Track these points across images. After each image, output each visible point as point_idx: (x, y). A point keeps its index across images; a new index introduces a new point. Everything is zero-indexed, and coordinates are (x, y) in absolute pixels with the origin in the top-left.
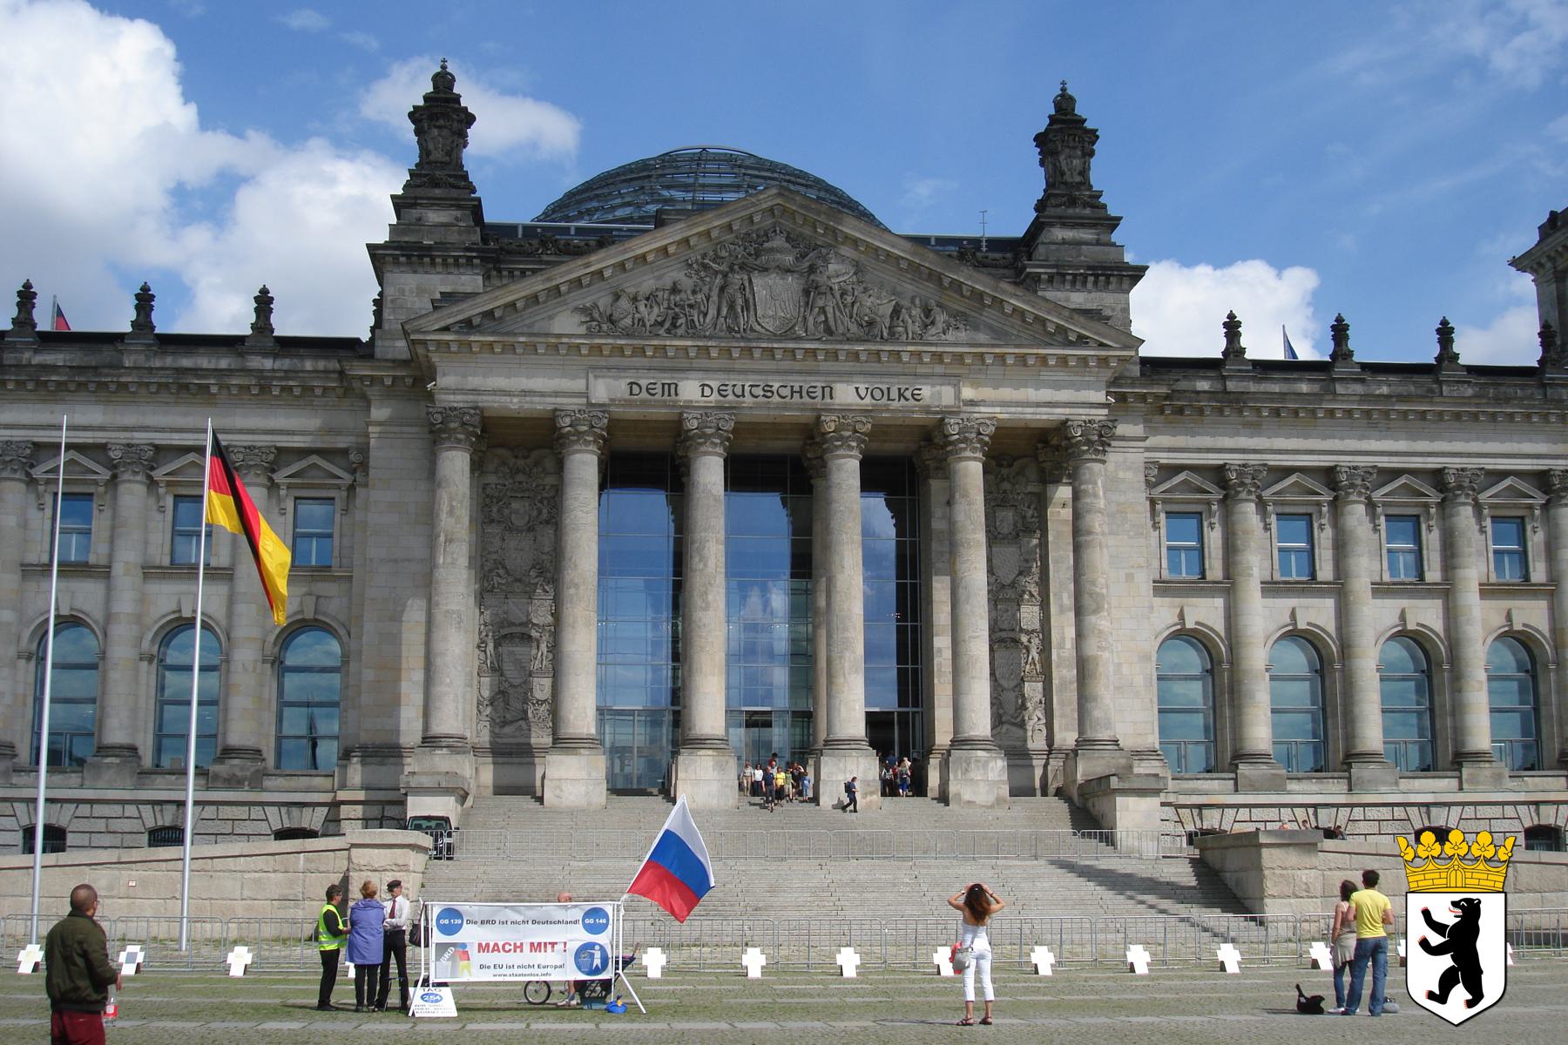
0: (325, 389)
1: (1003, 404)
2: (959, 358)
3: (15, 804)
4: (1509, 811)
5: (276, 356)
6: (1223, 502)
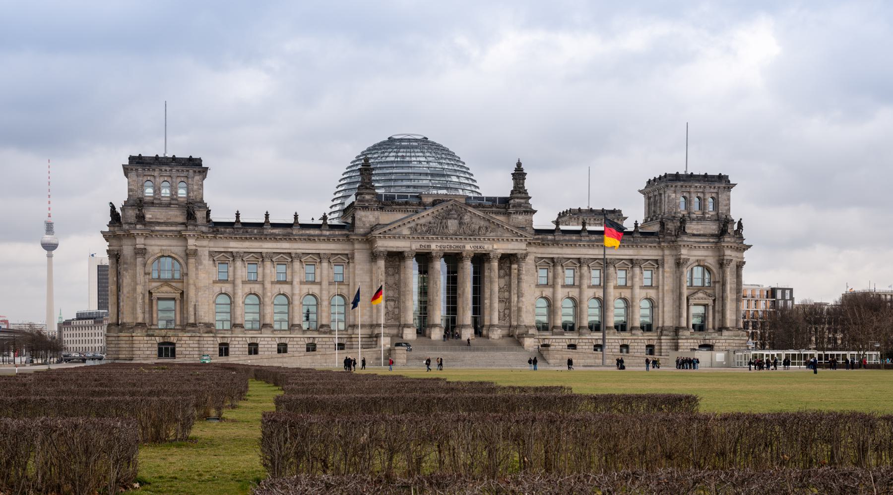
1: (503, 249)
2: (494, 239)
3: (276, 339)
4: (616, 341)
5: (329, 231)
6: (554, 266)
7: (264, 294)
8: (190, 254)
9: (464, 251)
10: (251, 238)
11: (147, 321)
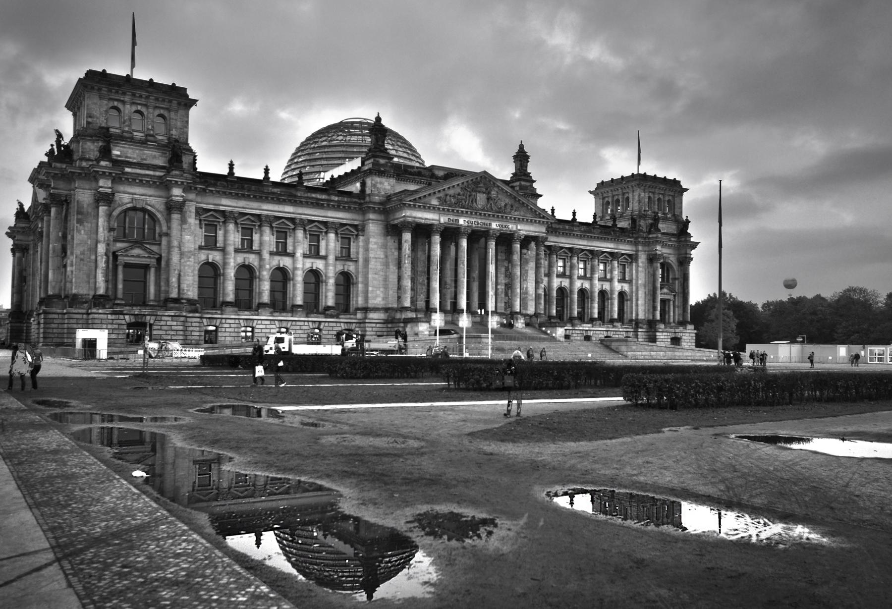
0: (355, 208)
1: (526, 231)
2: (519, 219)
5: (338, 196)
6: (549, 255)
7: (261, 267)
8: (172, 207)
9: (491, 229)
10: (249, 196)
11: (110, 293)
